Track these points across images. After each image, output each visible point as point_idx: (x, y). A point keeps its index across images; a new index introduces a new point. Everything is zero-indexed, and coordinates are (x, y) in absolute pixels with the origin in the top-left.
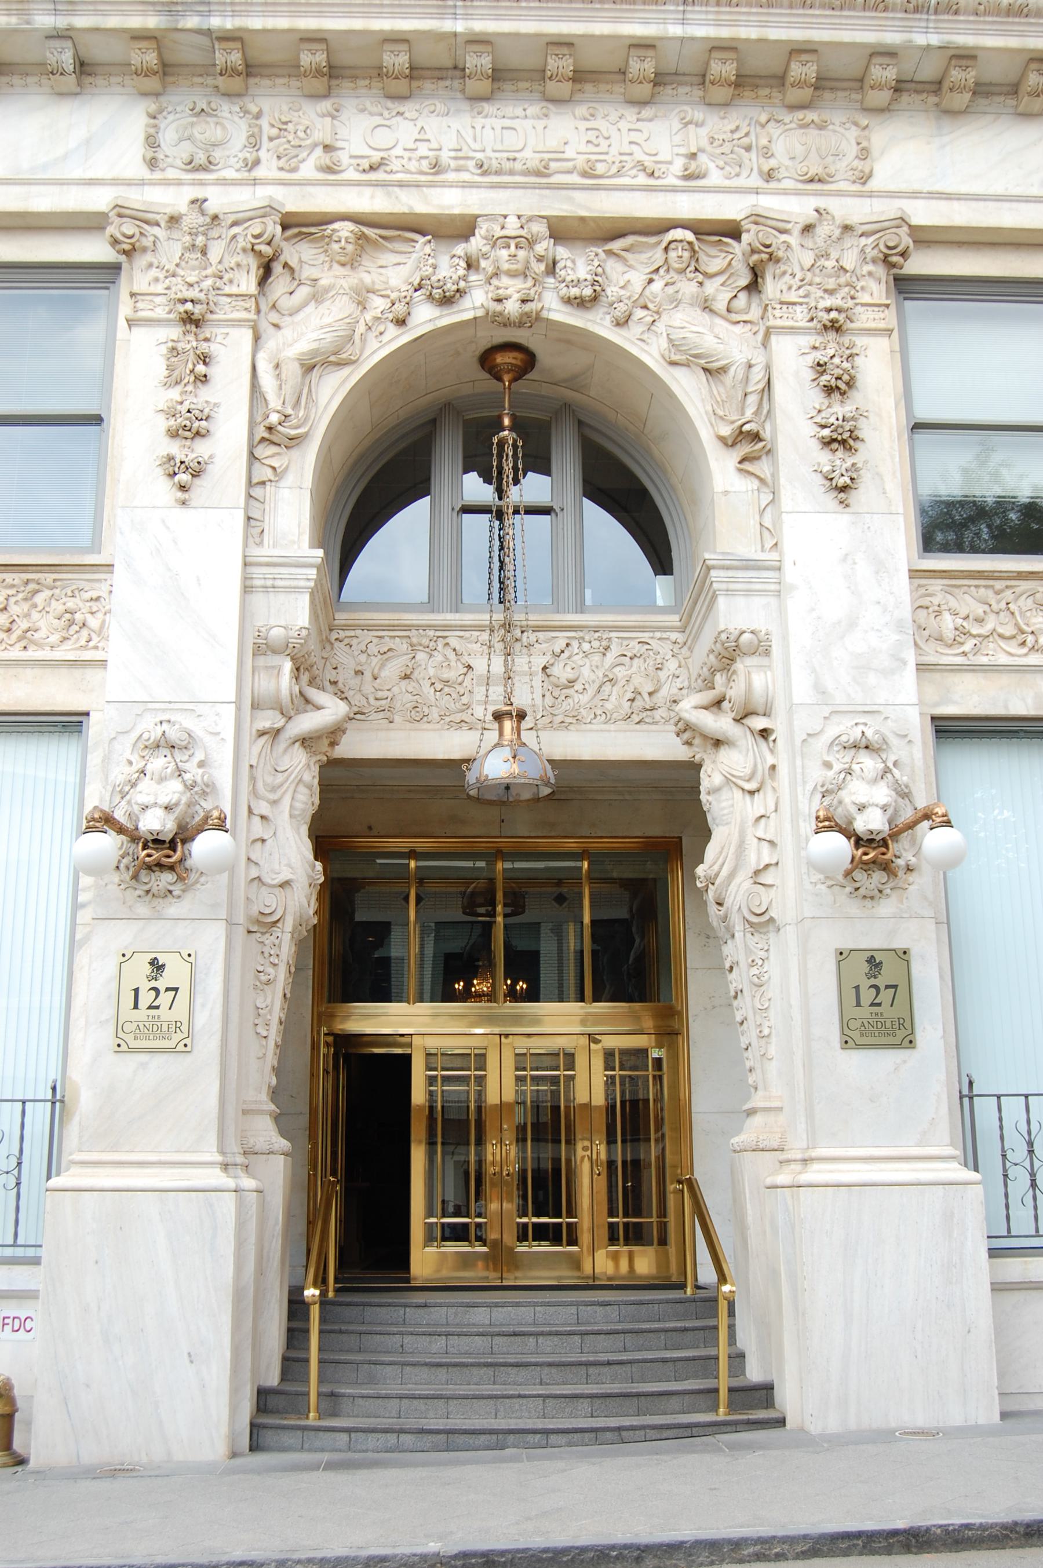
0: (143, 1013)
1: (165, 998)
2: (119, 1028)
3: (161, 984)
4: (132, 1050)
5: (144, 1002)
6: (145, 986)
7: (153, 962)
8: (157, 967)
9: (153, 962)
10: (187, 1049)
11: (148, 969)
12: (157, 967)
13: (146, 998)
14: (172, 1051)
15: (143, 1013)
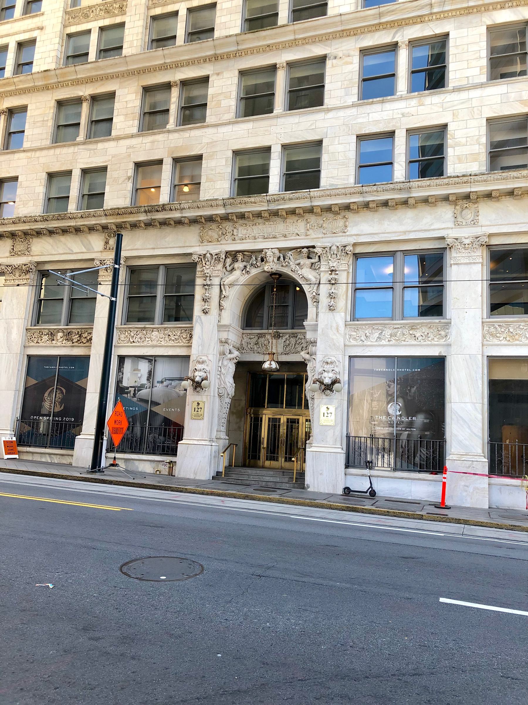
0: (196, 412)
1: (200, 409)
2: (191, 415)
3: (199, 407)
4: (194, 419)
5: (196, 411)
6: (196, 407)
7: (198, 403)
8: (198, 404)
9: (198, 403)
10: (203, 419)
11: (197, 404)
12: (198, 404)
13: (196, 410)
14: (200, 419)
15: (196, 412)
